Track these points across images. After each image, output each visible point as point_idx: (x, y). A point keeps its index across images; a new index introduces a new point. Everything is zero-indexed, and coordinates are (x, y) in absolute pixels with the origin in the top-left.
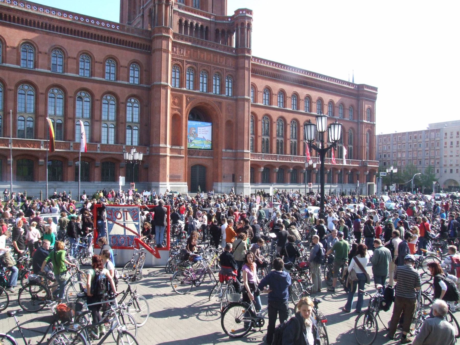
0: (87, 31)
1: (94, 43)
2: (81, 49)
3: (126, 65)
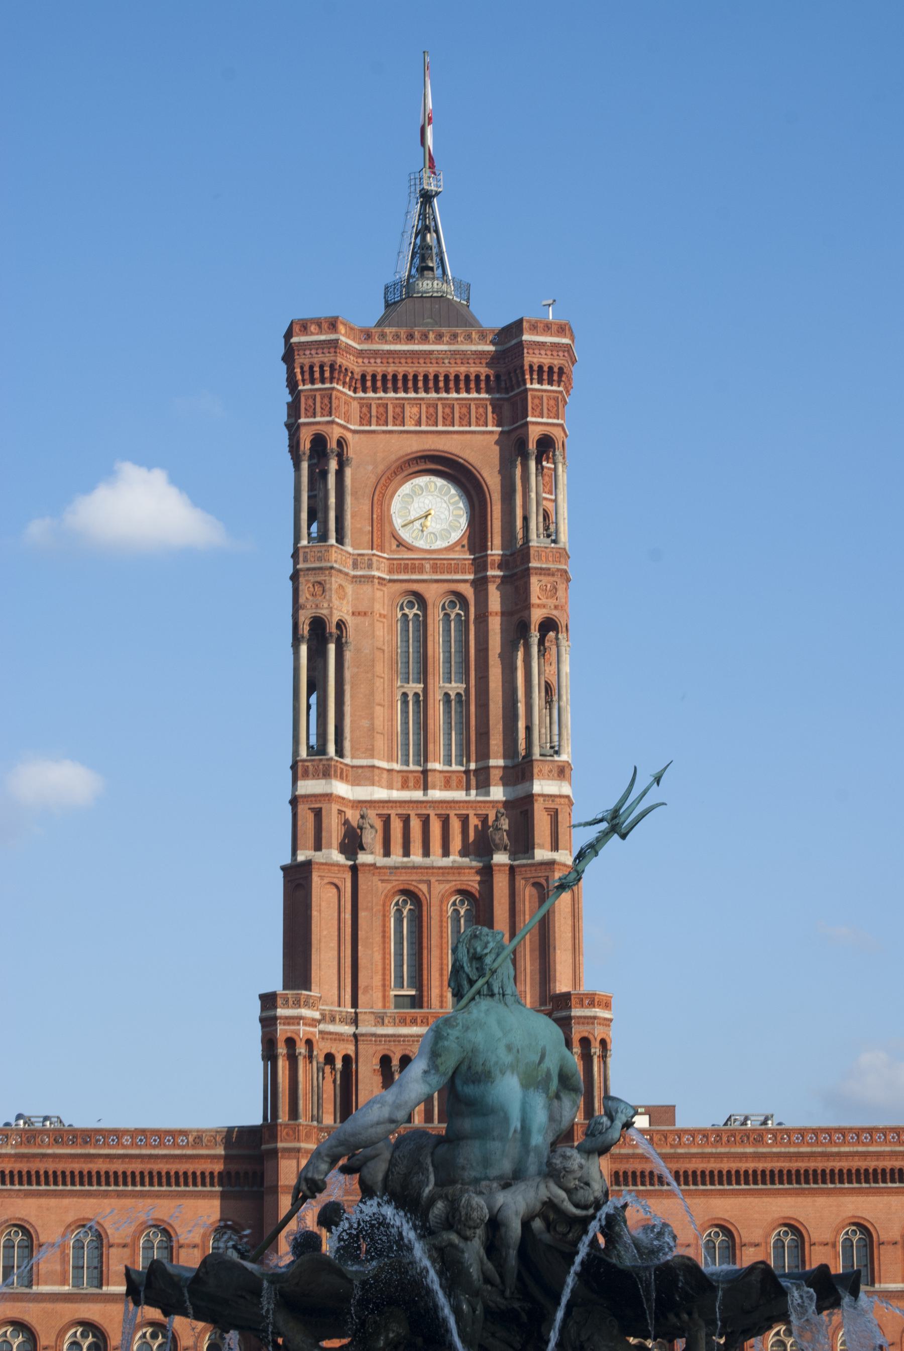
0: (86, 1167)
1: (106, 1195)
2: (70, 1218)
3: (197, 1240)
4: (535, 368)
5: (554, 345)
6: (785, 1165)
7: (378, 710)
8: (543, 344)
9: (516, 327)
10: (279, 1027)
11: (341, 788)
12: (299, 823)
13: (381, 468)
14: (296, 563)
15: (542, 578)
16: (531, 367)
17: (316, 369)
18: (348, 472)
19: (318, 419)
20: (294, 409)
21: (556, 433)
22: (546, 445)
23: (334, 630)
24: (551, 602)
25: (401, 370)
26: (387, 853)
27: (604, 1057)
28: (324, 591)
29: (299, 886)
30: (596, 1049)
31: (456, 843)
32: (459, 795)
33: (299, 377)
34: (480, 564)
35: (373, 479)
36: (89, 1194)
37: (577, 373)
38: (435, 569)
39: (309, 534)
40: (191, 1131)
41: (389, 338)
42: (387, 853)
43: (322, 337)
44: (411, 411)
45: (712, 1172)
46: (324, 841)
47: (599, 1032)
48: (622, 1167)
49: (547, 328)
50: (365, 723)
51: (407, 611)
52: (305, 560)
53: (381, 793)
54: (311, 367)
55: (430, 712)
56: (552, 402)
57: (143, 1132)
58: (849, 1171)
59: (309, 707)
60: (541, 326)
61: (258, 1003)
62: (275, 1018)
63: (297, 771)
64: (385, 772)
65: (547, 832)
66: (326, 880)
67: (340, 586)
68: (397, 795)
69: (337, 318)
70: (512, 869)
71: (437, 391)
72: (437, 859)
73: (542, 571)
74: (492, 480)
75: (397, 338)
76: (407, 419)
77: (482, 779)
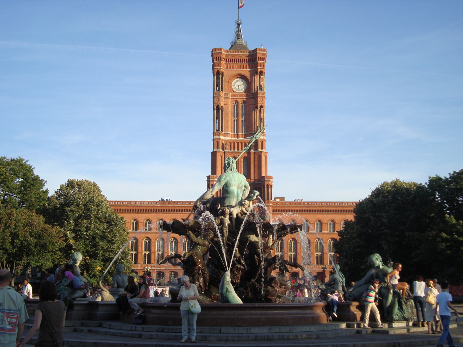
0: (174, 208)
1: (178, 213)
4: (259, 58)
5: (263, 53)
6: (305, 209)
7: (229, 123)
8: (261, 53)
9: (256, 50)
10: (210, 182)
11: (222, 137)
12: (214, 144)
13: (230, 77)
14: (214, 95)
15: (261, 98)
16: (258, 58)
17: (218, 58)
18: (224, 78)
19: (218, 67)
20: (213, 66)
21: (263, 70)
22: (261, 72)
23: (221, 108)
24: (262, 102)
25: (234, 58)
26: (231, 149)
27: (271, 188)
28: (219, 100)
29: (214, 156)
30: (270, 187)
33: (214, 59)
35: (228, 79)
36: (175, 213)
37: (267, 59)
39: (216, 90)
40: (194, 201)
41: (232, 52)
42: (231, 149)
43: (219, 52)
45: (291, 210)
46: (219, 147)
47: (270, 183)
48: (274, 209)
49: (262, 50)
50: (227, 125)
51: (235, 104)
52: (215, 94)
53: (230, 138)
54: (217, 58)
55: (239, 123)
56: (262, 64)
57: (185, 202)
58: (317, 210)
59: (216, 122)
60: (260, 50)
62: (210, 180)
64: (230, 135)
65: (261, 146)
66: (219, 155)
67: (222, 99)
68: (232, 139)
69: (221, 48)
70: (254, 153)
71: (240, 62)
73: (260, 97)
75: (233, 52)
76: (235, 68)
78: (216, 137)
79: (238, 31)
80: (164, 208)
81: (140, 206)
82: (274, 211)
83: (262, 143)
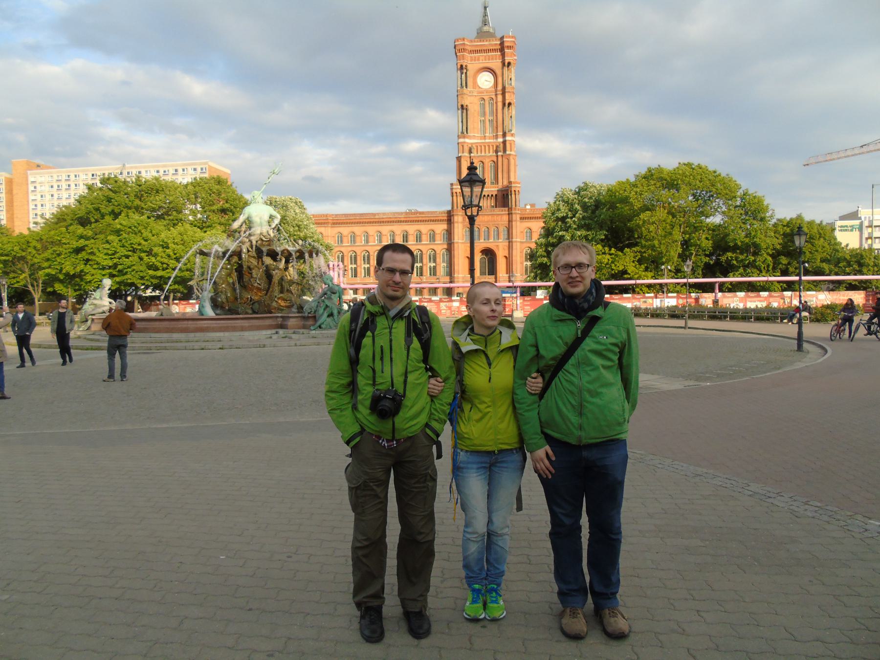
8: (508, 41)
18: (468, 72)
21: (512, 62)
30: (517, 193)
31: (491, 151)
32: (492, 141)
34: (496, 91)
38: (487, 92)
44: (481, 58)
47: (517, 189)
48: (523, 216)
61: (450, 185)
63: (459, 137)
72: (487, 154)
74: (499, 72)
75: (478, 42)
77: (497, 137)
78: (461, 140)
79: (485, 15)
80: (408, 219)
81: (383, 218)
82: (521, 218)
83: (511, 144)
